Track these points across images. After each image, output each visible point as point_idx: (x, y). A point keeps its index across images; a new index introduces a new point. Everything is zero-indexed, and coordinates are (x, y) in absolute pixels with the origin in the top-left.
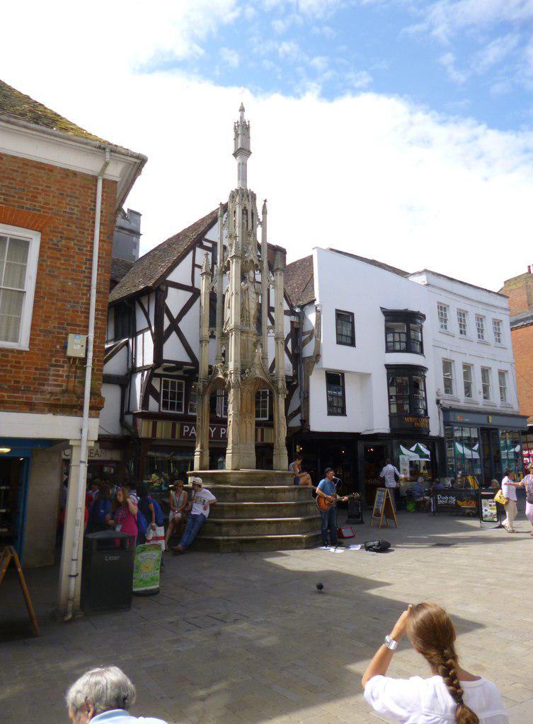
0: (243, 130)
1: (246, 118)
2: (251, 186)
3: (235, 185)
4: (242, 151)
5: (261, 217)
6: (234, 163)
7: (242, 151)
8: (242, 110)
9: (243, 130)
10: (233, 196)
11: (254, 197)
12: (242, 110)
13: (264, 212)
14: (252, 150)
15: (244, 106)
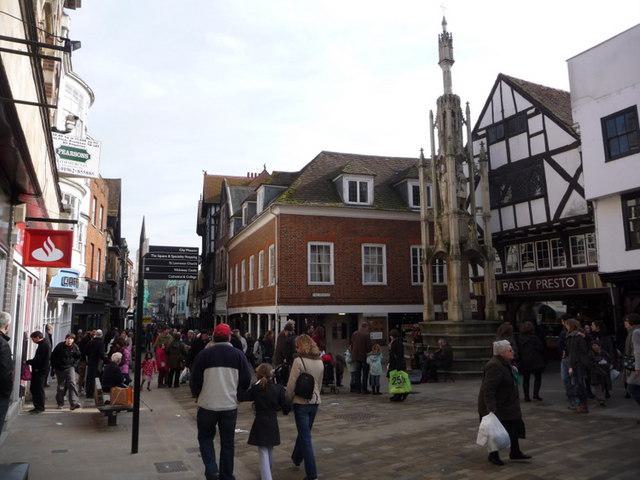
0: (446, 41)
1: (448, 30)
2: (455, 91)
3: (442, 93)
4: (447, 61)
5: (465, 116)
6: (439, 71)
7: (447, 61)
8: (444, 23)
9: (446, 41)
10: (441, 101)
11: (459, 101)
12: (444, 23)
13: (468, 112)
14: (455, 56)
15: (446, 19)
